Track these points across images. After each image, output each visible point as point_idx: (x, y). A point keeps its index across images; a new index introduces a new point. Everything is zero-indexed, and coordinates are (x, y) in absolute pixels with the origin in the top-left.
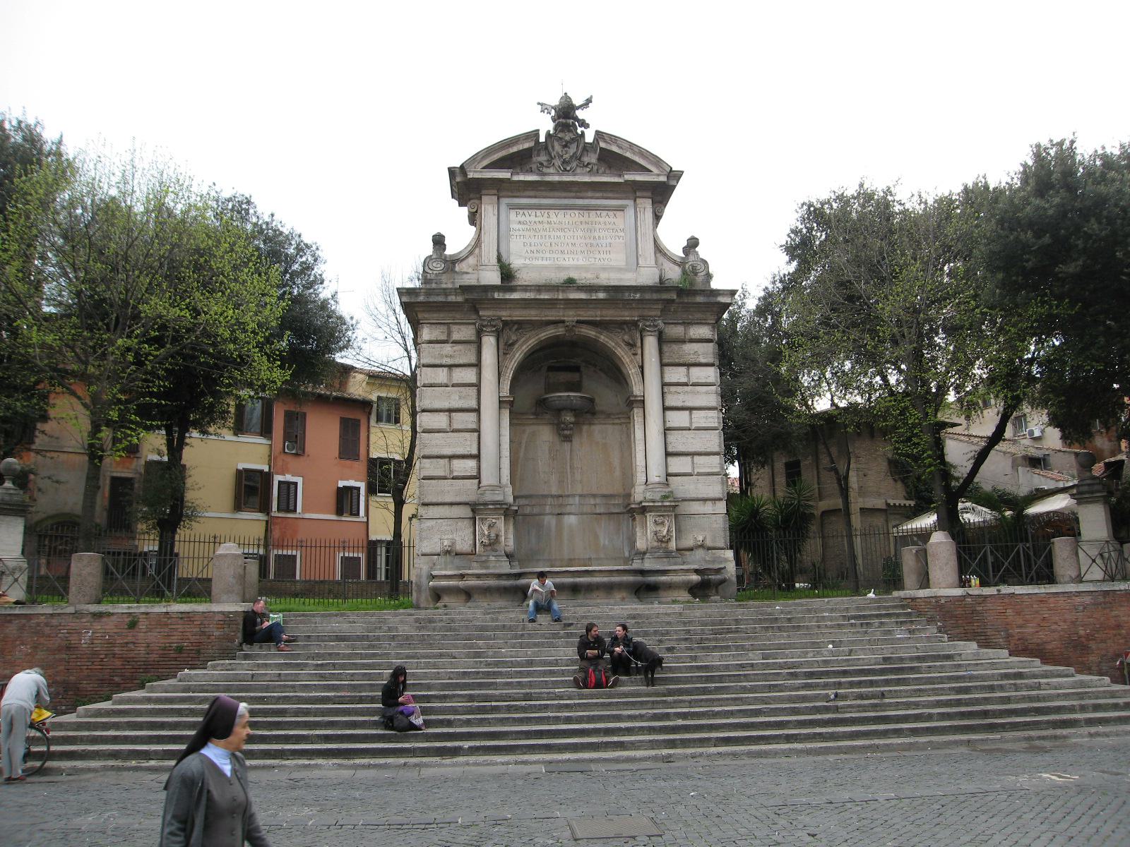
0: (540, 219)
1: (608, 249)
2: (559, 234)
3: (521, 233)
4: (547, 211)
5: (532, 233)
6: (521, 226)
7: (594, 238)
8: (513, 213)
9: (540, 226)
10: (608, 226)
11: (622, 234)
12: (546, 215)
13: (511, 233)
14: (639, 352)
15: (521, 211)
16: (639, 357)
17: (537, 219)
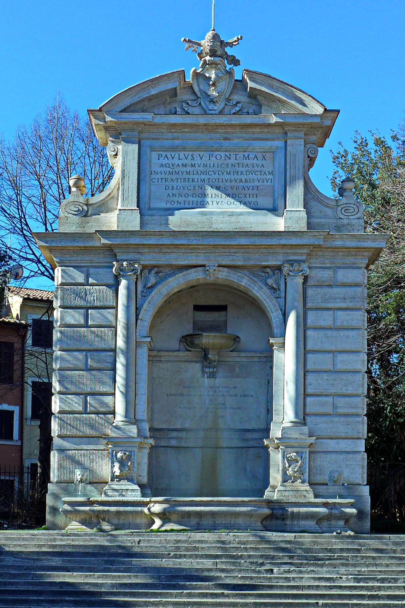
0: (185, 162)
1: (255, 192)
2: (203, 177)
3: (163, 176)
4: (191, 153)
5: (174, 177)
6: (162, 169)
7: (241, 181)
8: (155, 155)
9: (184, 169)
10: (256, 169)
11: (271, 177)
12: (190, 157)
13: (153, 176)
14: (283, 295)
15: (164, 154)
16: (282, 301)
17: (180, 162)
